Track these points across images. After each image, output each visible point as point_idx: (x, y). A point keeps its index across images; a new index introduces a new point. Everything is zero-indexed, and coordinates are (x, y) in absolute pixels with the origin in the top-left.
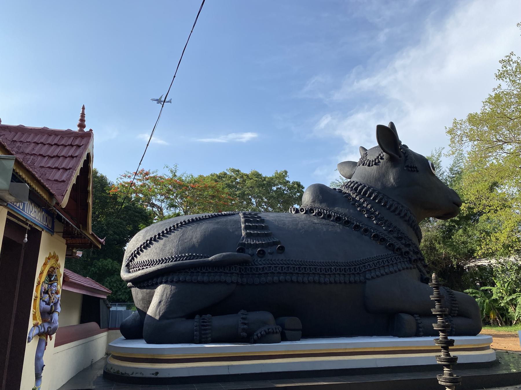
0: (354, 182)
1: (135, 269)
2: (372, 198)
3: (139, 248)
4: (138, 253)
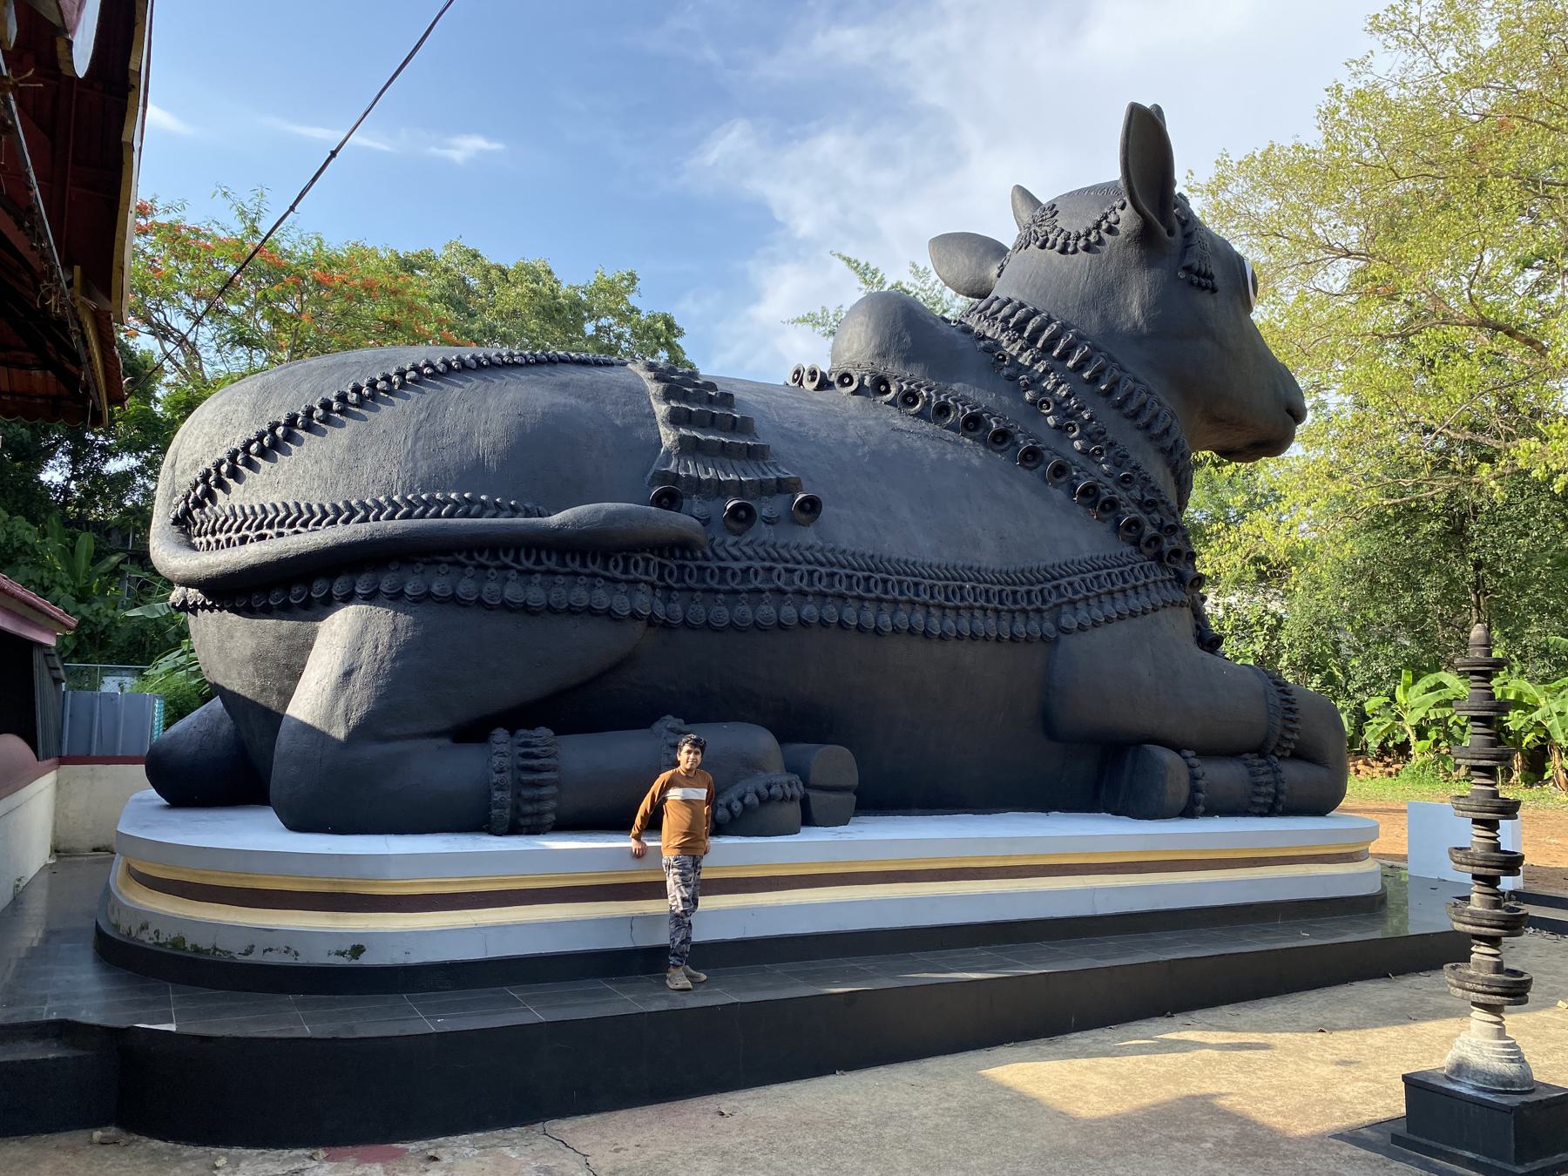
0: (1010, 301)
1: (222, 537)
2: (1070, 364)
3: (236, 452)
4: (235, 474)
